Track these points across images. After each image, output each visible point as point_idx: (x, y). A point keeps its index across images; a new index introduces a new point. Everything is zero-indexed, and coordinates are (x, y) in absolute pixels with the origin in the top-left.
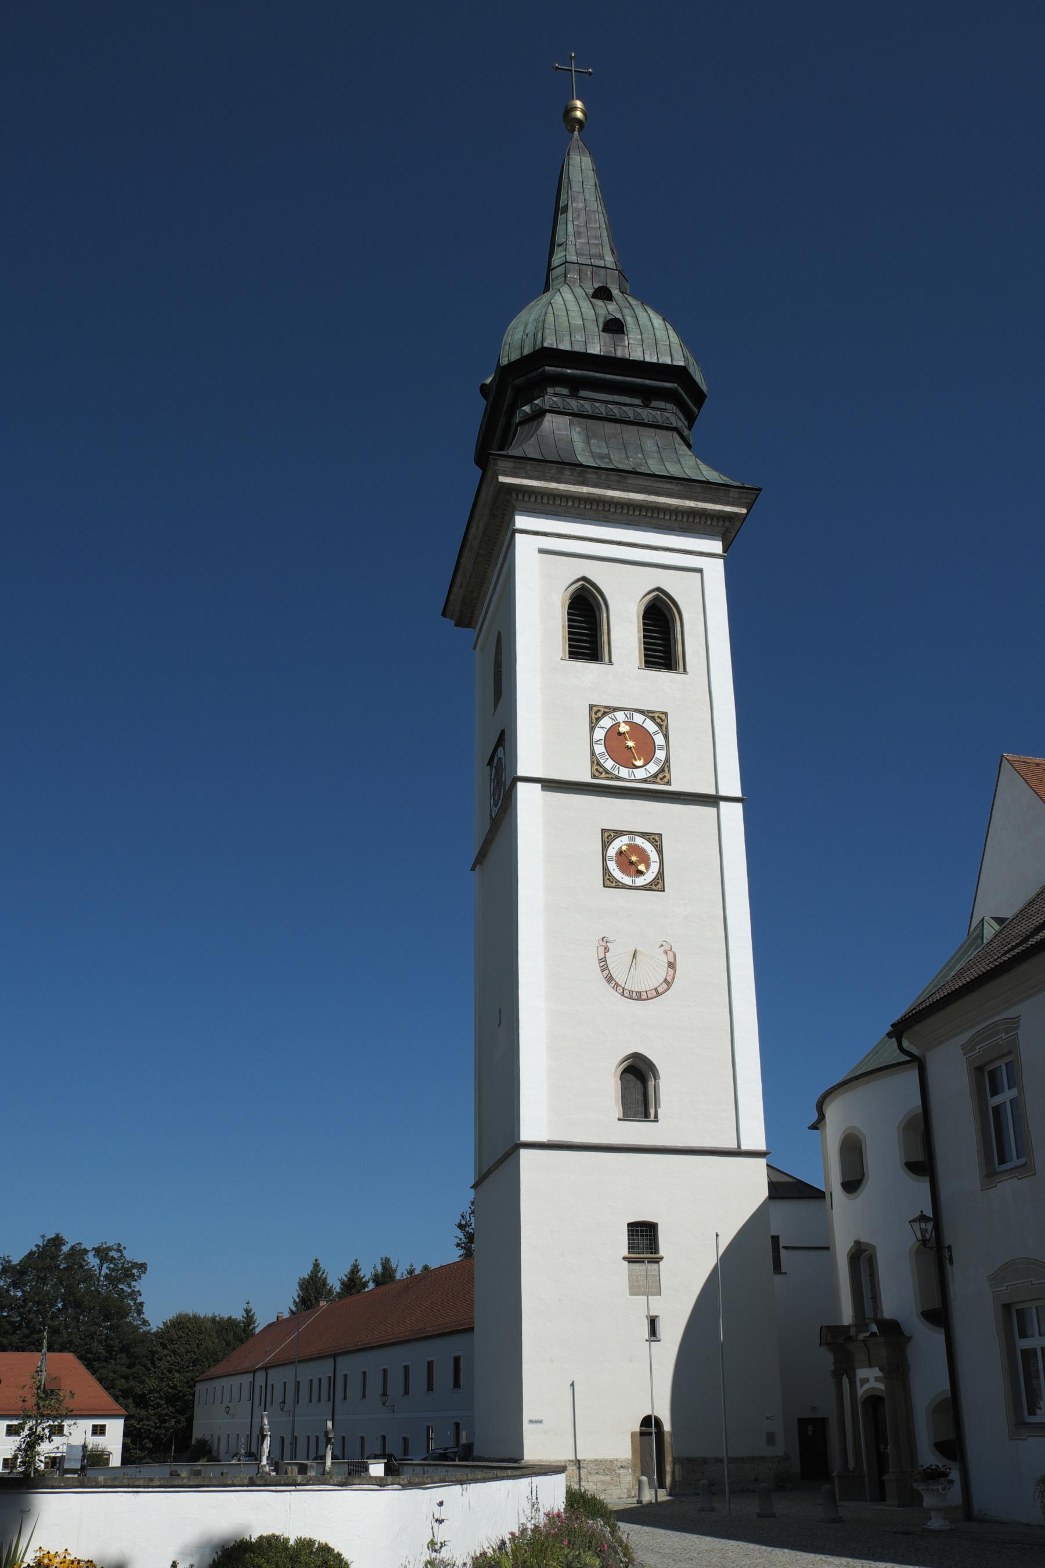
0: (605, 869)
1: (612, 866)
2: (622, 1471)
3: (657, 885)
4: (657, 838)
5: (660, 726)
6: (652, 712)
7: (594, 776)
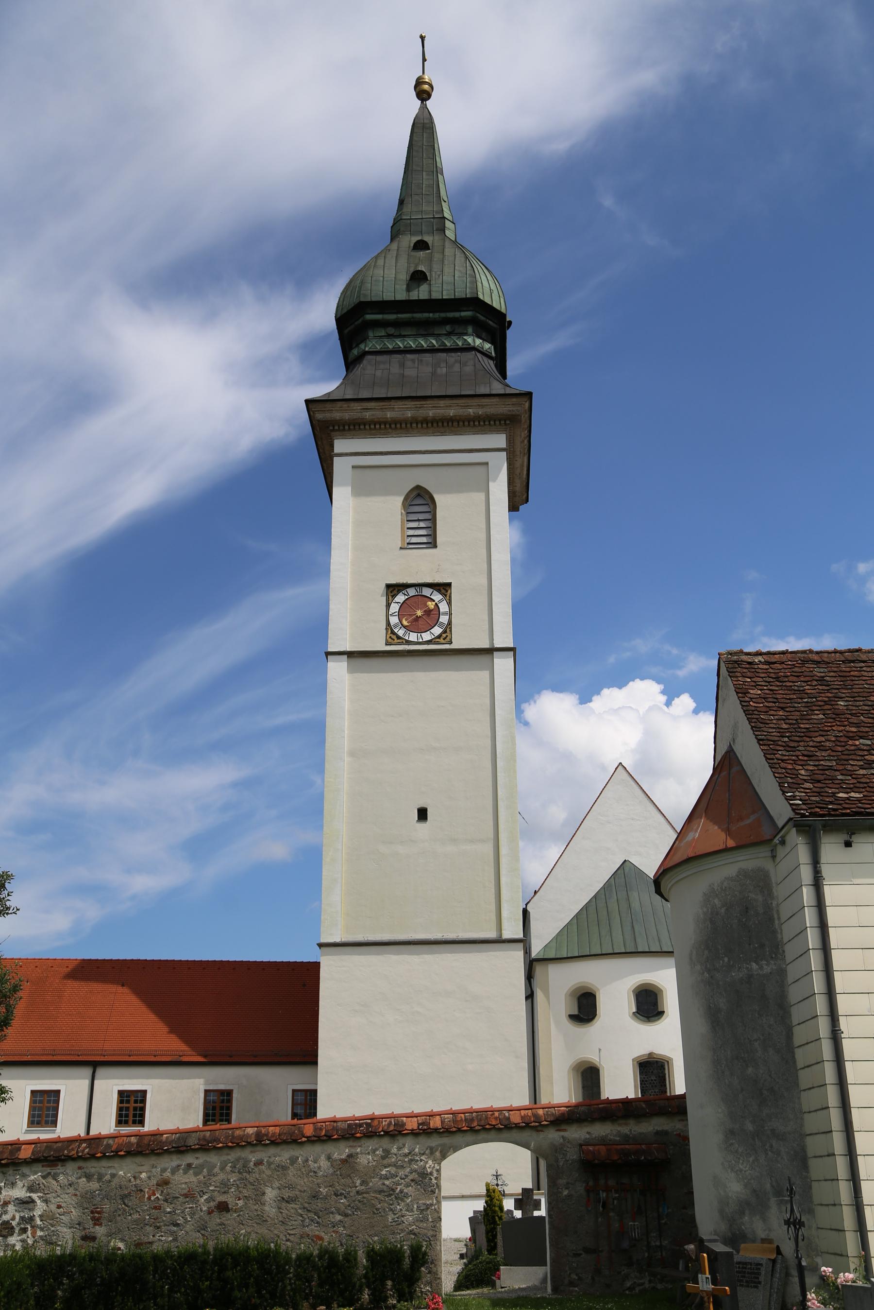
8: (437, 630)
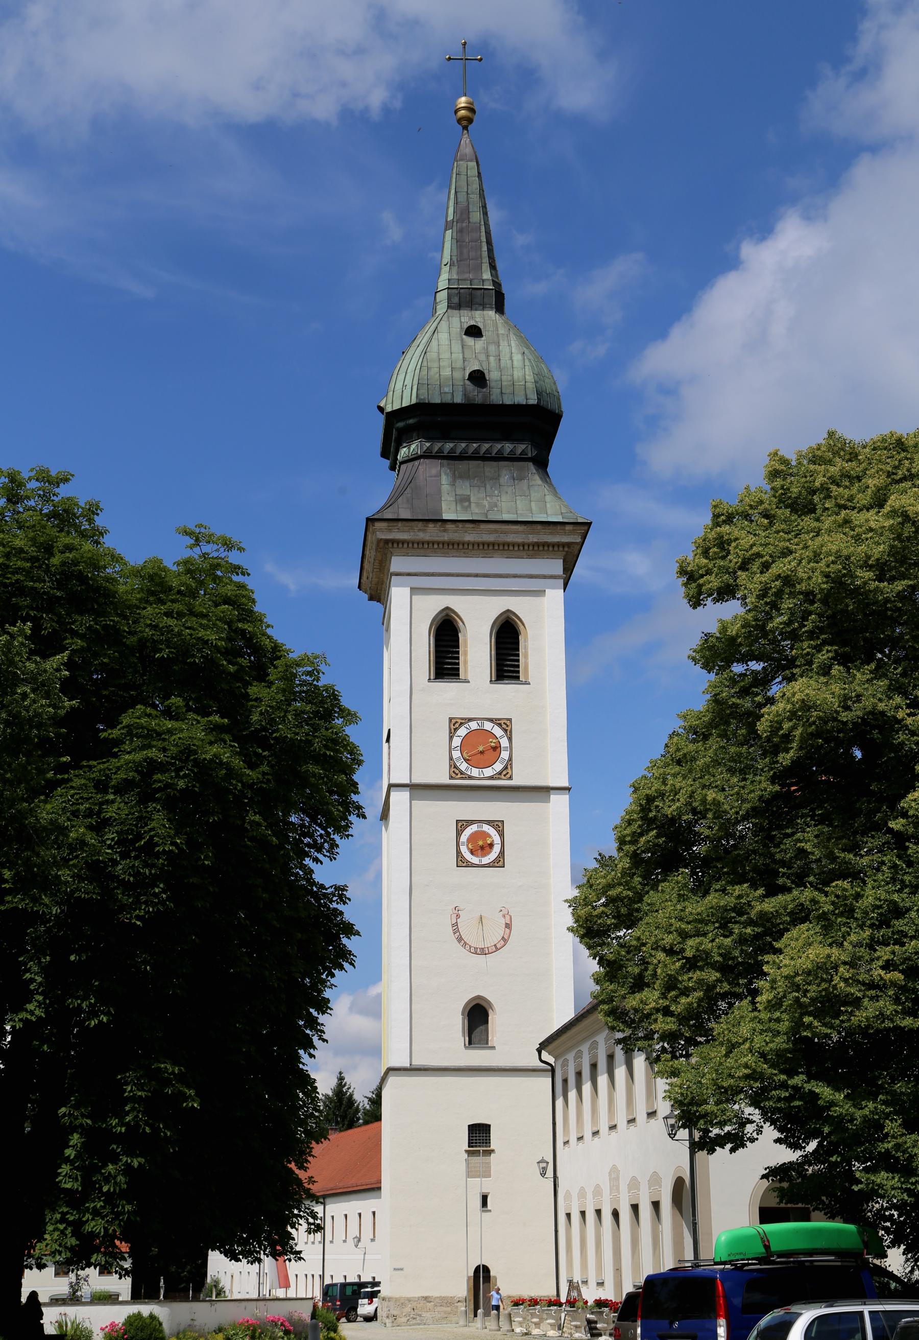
0: (459, 852)
2: (459, 1304)
3: (499, 862)
4: (500, 824)
5: (505, 731)
6: (499, 720)
7: (451, 778)
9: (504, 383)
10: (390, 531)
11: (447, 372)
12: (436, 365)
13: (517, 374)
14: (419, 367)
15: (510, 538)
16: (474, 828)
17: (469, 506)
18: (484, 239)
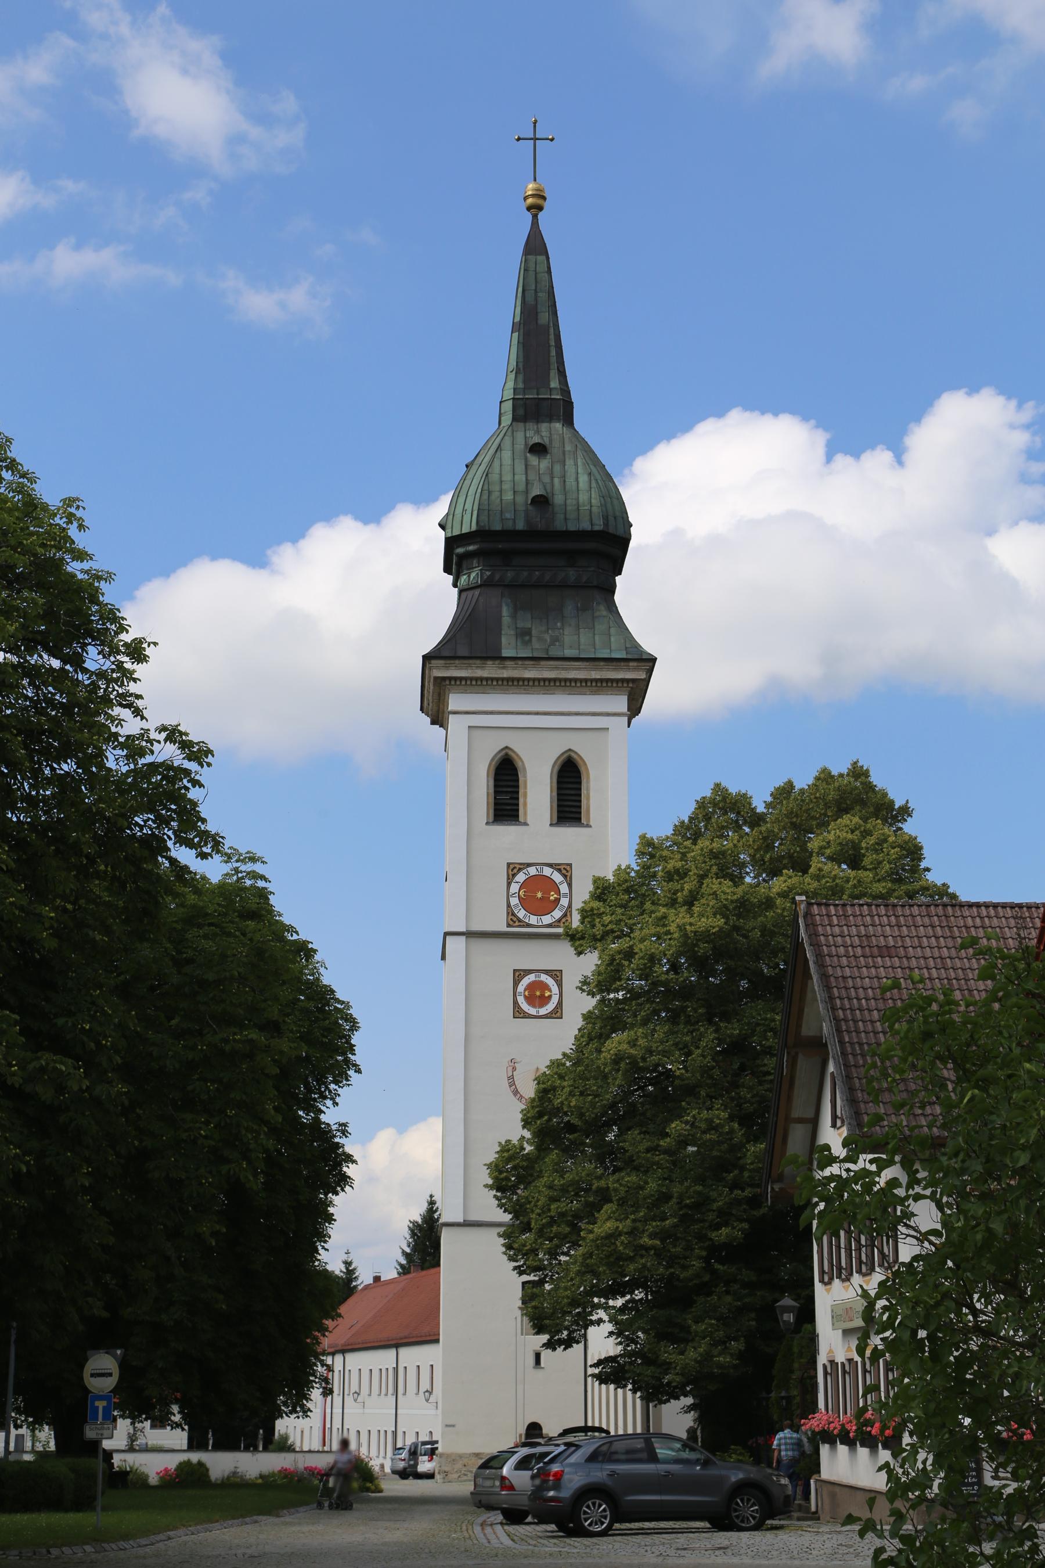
1: (521, 1000)
5: (565, 876)
7: (509, 926)
8: (557, 914)
9: (569, 508)
10: (447, 667)
11: (508, 496)
12: (497, 488)
13: (583, 497)
14: (479, 490)
15: (572, 675)
16: (532, 977)
17: (530, 641)
18: (552, 343)
